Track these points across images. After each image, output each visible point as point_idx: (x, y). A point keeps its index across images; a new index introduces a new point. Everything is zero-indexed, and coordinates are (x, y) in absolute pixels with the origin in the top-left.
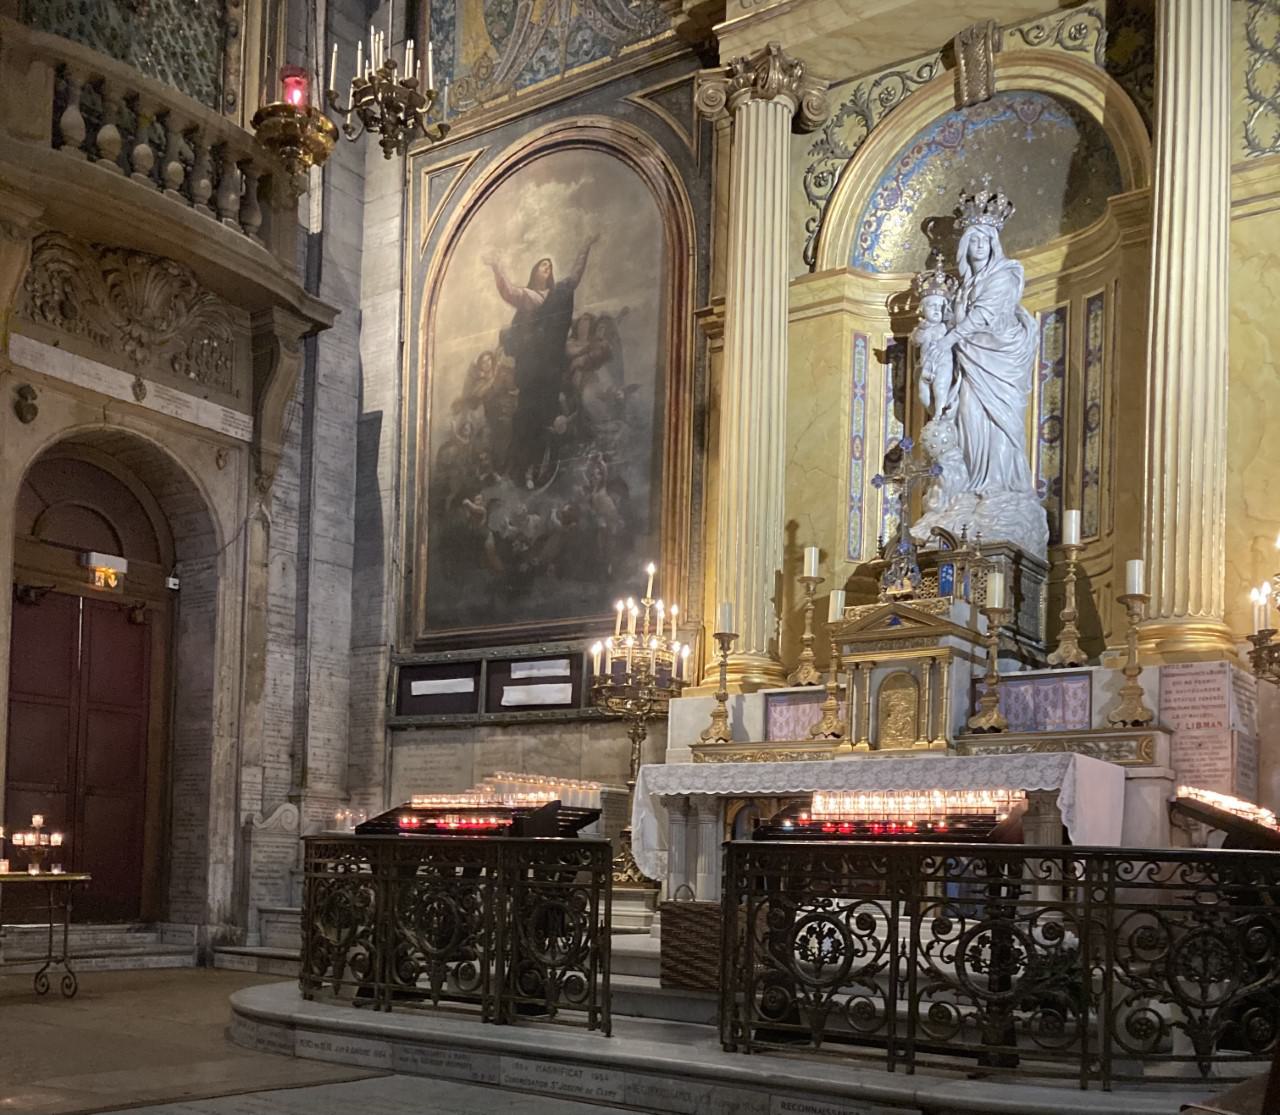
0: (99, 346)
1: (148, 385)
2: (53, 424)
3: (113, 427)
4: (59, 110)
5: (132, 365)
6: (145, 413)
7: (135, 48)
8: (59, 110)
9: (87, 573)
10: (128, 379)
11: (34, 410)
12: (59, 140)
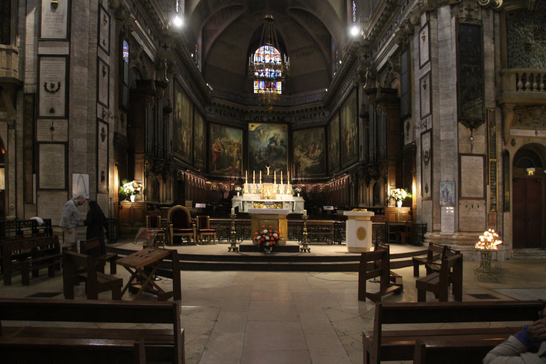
0: (527, 126)
1: (538, 131)
2: (519, 144)
3: (531, 142)
4: (517, 82)
5: (535, 128)
6: (539, 138)
7: (531, 59)
8: (517, 82)
9: (527, 173)
10: (534, 132)
11: (515, 143)
12: (517, 89)
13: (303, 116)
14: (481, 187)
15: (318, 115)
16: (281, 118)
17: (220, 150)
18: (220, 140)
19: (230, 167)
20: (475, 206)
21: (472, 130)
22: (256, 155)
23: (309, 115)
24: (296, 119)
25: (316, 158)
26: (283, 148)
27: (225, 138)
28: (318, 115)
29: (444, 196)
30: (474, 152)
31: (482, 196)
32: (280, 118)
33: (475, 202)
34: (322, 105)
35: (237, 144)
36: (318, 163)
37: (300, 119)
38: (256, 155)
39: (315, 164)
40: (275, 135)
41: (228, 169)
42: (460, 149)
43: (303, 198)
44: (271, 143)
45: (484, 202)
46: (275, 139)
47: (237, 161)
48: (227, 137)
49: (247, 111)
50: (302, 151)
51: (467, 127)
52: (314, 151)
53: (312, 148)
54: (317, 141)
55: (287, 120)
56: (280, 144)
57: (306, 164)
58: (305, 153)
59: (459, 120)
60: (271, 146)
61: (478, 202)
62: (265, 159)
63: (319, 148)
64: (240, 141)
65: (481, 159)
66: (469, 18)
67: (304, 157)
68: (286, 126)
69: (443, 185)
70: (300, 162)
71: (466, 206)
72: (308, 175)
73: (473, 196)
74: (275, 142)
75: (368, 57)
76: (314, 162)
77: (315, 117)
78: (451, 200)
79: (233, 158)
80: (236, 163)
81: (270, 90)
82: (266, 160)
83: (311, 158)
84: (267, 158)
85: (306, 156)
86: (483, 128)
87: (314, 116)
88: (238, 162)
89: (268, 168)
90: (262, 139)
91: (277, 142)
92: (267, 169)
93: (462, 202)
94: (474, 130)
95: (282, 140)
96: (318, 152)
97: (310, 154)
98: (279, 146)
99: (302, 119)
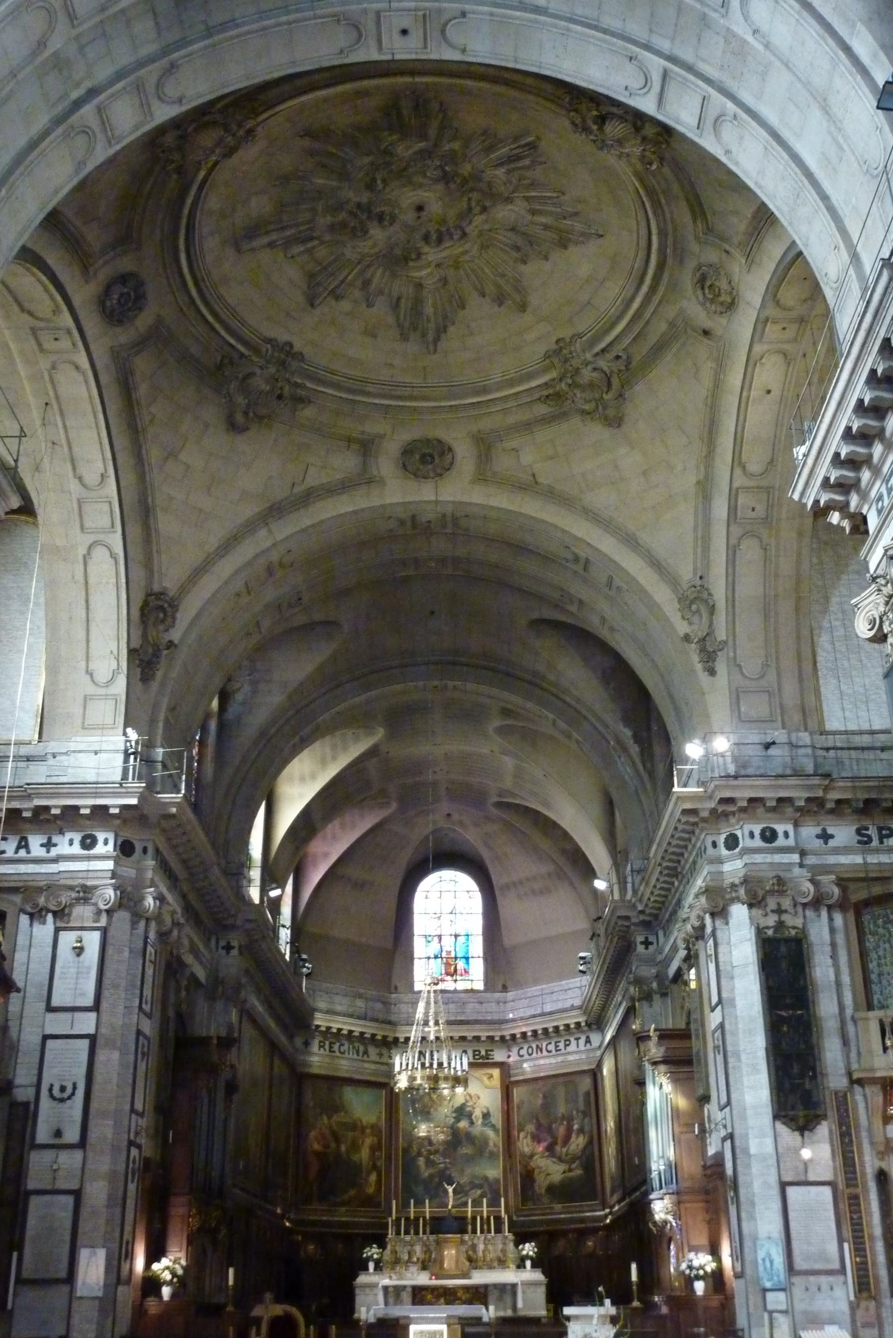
13: (537, 1046)
14: (832, 1247)
15: (573, 1042)
16: (483, 1053)
17: (326, 1146)
18: (329, 1118)
19: (352, 1192)
20: (824, 1287)
21: (802, 1135)
22: (419, 1154)
23: (553, 1043)
24: (522, 1052)
25: (573, 1160)
26: (490, 1133)
27: (343, 1114)
28: (573, 1042)
29: (765, 1269)
30: (812, 1177)
31: (836, 1265)
32: (480, 1052)
33: (824, 1280)
34: (582, 1019)
35: (373, 1127)
36: (579, 1172)
37: (530, 1055)
38: (419, 1154)
39: (571, 1174)
40: (468, 1098)
41: (346, 1197)
42: (782, 1172)
43: (544, 1273)
44: (458, 1120)
45: (841, 1278)
46: (468, 1109)
47: (369, 1174)
48: (346, 1112)
49: (396, 1040)
50: (536, 1139)
51: (794, 1130)
52: (567, 1140)
53: (562, 1131)
54: (574, 1113)
55: (499, 1056)
56: (480, 1121)
57: (548, 1174)
58: (544, 1144)
59: (776, 1117)
60: (458, 1128)
61: (831, 1279)
62: (442, 1165)
63: (581, 1131)
64: (379, 1117)
65: (827, 1191)
66: (780, 925)
67: (542, 1157)
68: (496, 1072)
69: (763, 1245)
70: (533, 1170)
71: (807, 1289)
72: (558, 1207)
73: (817, 1266)
74: (469, 1116)
75: (651, 943)
76: (570, 1170)
77: (569, 1049)
78: (778, 1276)
79: (361, 1164)
80: (366, 1180)
81: (456, 981)
82: (446, 1168)
83: (561, 1160)
84: (447, 1160)
85: (547, 1154)
86: (823, 1129)
87: (566, 1046)
88: (373, 1177)
89: (450, 1190)
90: (436, 1110)
91: (473, 1117)
92: (446, 1192)
93: (796, 1280)
94: (806, 1133)
95: (485, 1111)
96: (578, 1143)
97: (558, 1148)
98: (478, 1128)
99: (534, 1055)
